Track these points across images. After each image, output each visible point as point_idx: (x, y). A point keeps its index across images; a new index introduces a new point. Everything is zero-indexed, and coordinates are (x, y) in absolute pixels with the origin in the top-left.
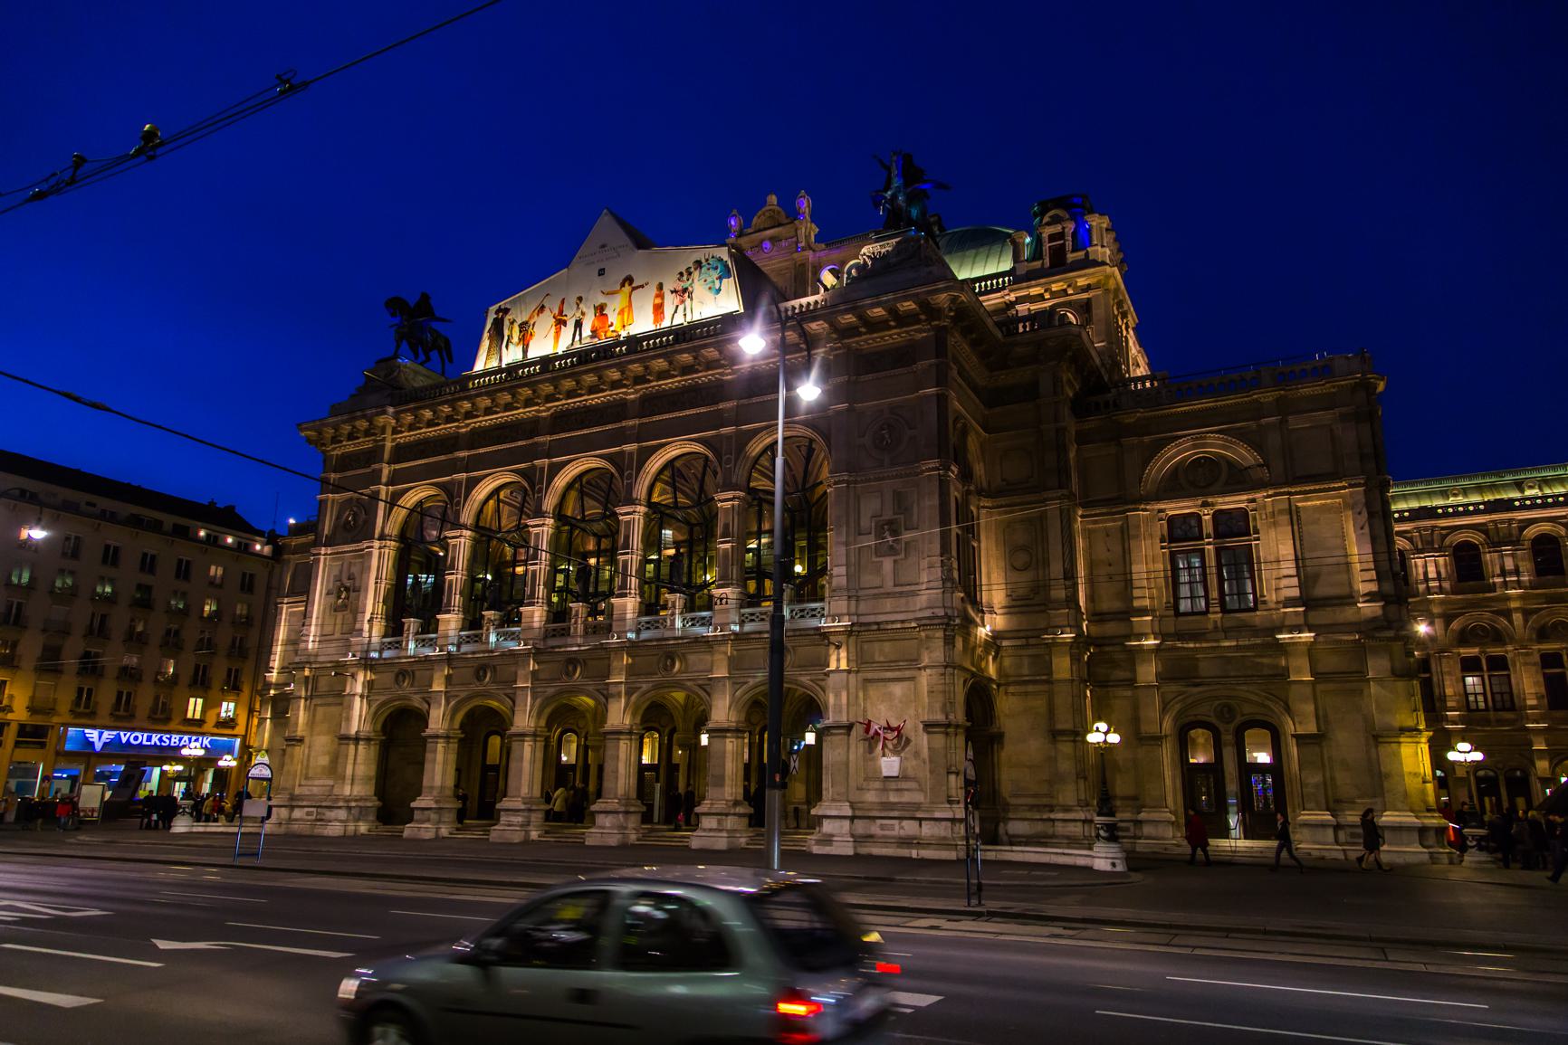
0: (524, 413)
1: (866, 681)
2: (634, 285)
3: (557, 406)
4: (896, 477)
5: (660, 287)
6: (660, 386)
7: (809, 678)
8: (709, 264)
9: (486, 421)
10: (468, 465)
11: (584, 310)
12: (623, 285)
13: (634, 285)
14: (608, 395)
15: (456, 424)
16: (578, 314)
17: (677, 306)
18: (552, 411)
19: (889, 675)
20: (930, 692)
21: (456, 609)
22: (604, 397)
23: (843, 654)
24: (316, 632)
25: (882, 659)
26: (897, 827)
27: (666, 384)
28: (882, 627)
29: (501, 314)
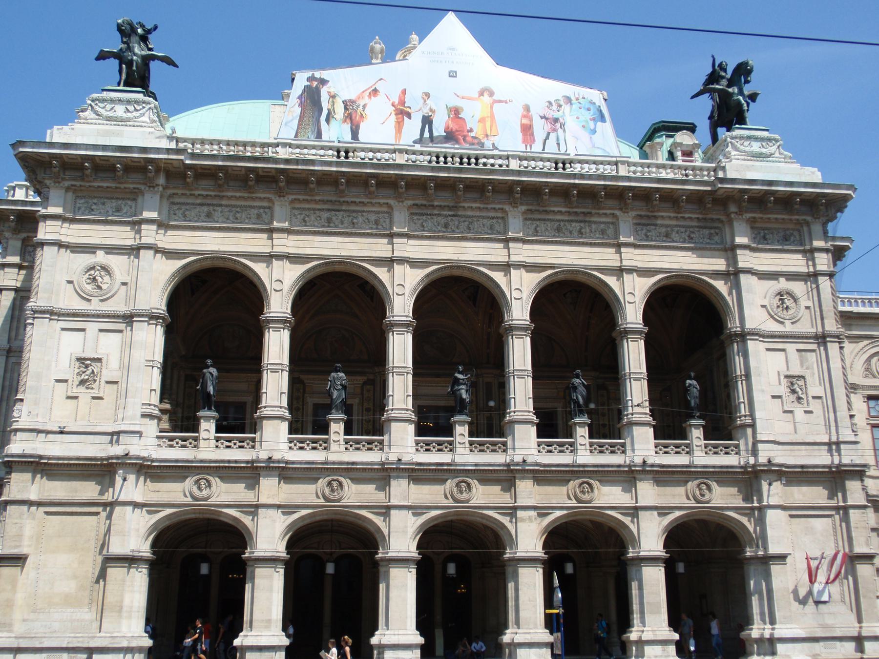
2: (495, 97)
5: (527, 108)
8: (580, 103)
12: (481, 94)
13: (495, 97)
16: (426, 111)
17: (549, 134)
29: (315, 84)
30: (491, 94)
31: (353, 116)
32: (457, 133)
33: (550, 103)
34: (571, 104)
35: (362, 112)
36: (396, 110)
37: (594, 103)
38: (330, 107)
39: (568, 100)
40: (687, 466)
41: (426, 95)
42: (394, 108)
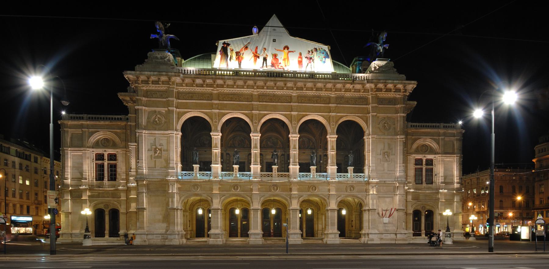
0: (246, 91)
1: (379, 197)
3: (262, 91)
4: (388, 139)
5: (301, 54)
6: (306, 93)
7: (361, 195)
8: (320, 51)
9: (227, 90)
10: (219, 107)
11: (267, 54)
12: (284, 49)
13: (289, 50)
14: (284, 92)
15: (212, 88)
16: (265, 55)
17: (308, 64)
18: (259, 93)
19: (386, 196)
20: (399, 201)
21: (219, 163)
22: (283, 92)
23: (375, 189)
24: (145, 166)
25: (383, 191)
26: (389, 236)
27: (309, 93)
28: (385, 182)
29: (225, 45)
30: (288, 48)
31: (239, 57)
32: (275, 64)
33: (309, 51)
34: (317, 51)
35: (242, 56)
36: (254, 55)
37: (325, 51)
38: (231, 55)
39: (316, 50)
40: (347, 181)
41: (265, 49)
42: (253, 55)
